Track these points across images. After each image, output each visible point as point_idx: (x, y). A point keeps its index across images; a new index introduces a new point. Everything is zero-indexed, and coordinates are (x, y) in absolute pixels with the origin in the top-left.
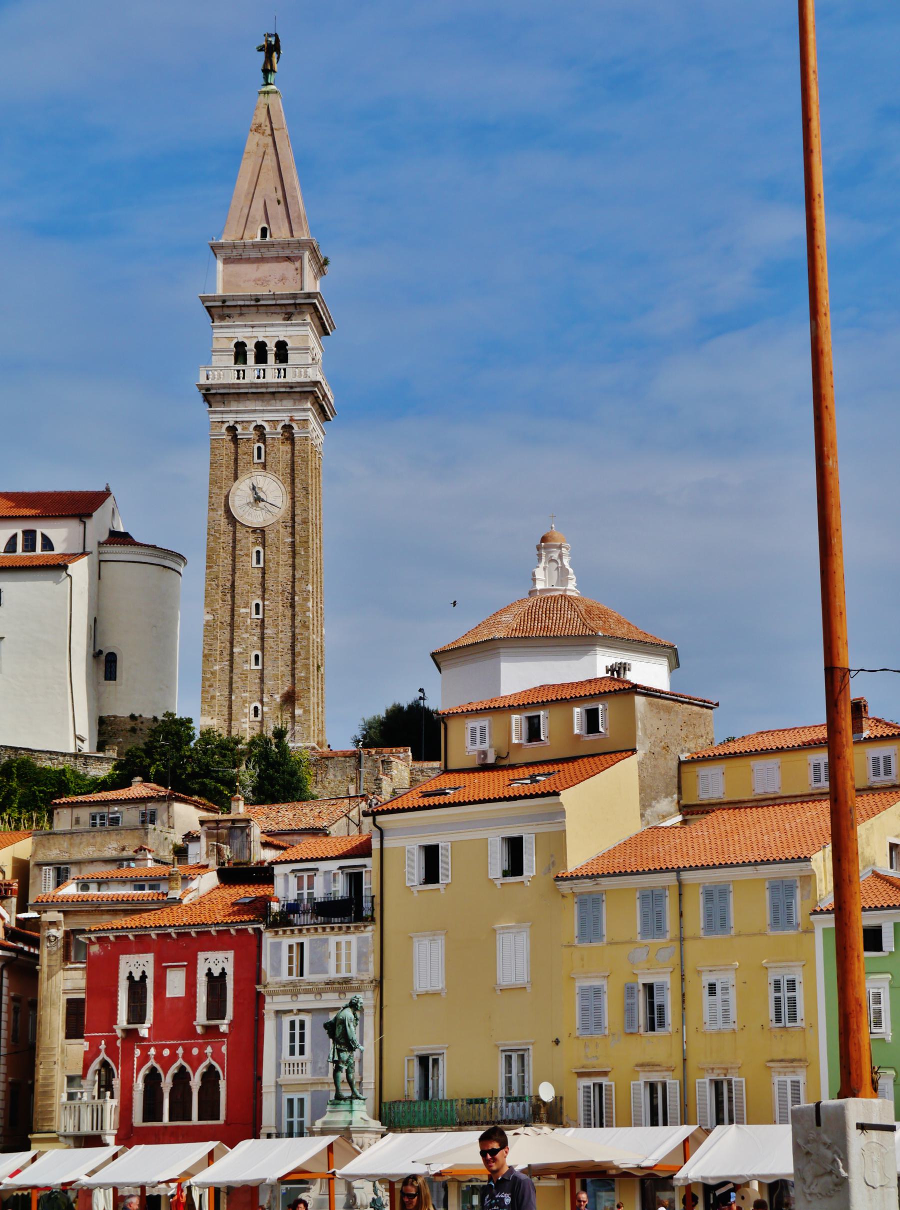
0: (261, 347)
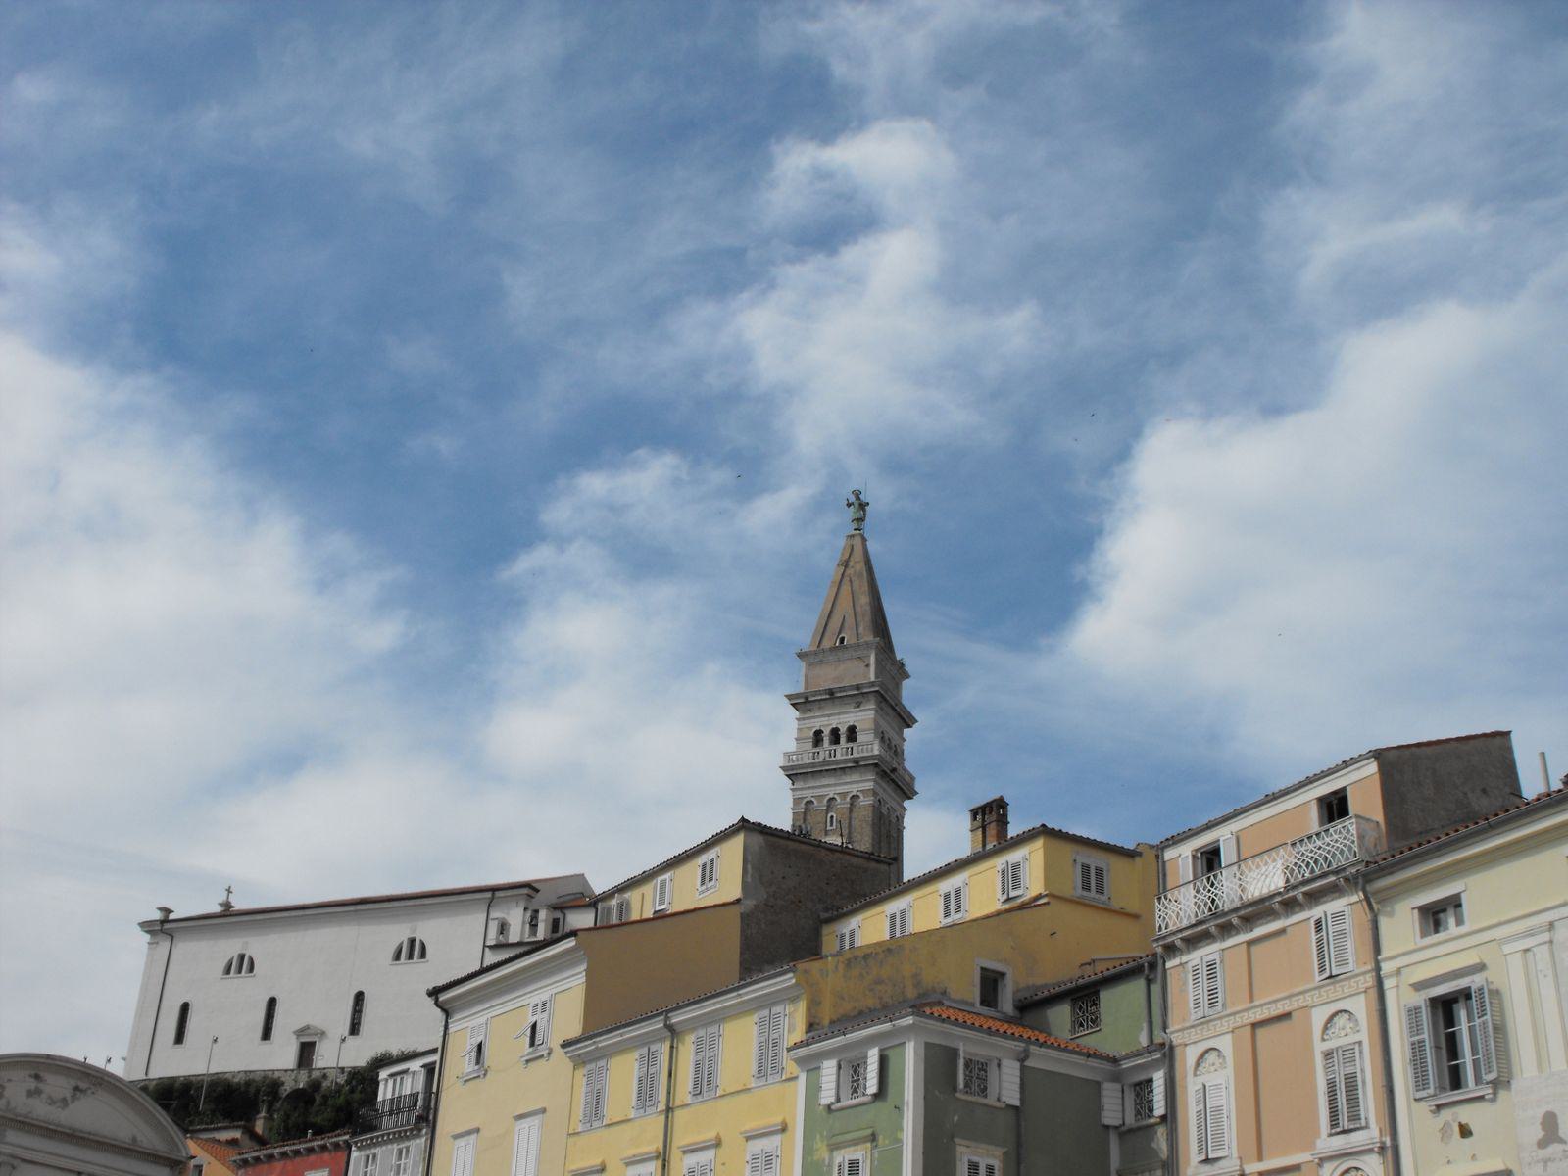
0: (835, 733)
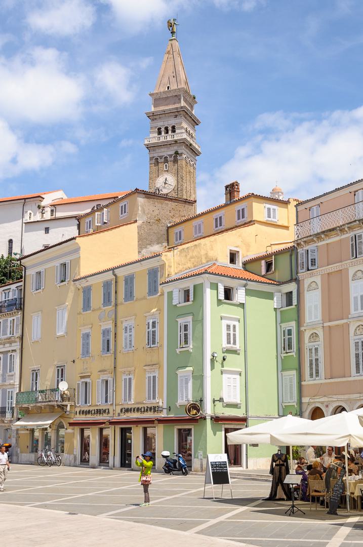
0: (166, 129)
